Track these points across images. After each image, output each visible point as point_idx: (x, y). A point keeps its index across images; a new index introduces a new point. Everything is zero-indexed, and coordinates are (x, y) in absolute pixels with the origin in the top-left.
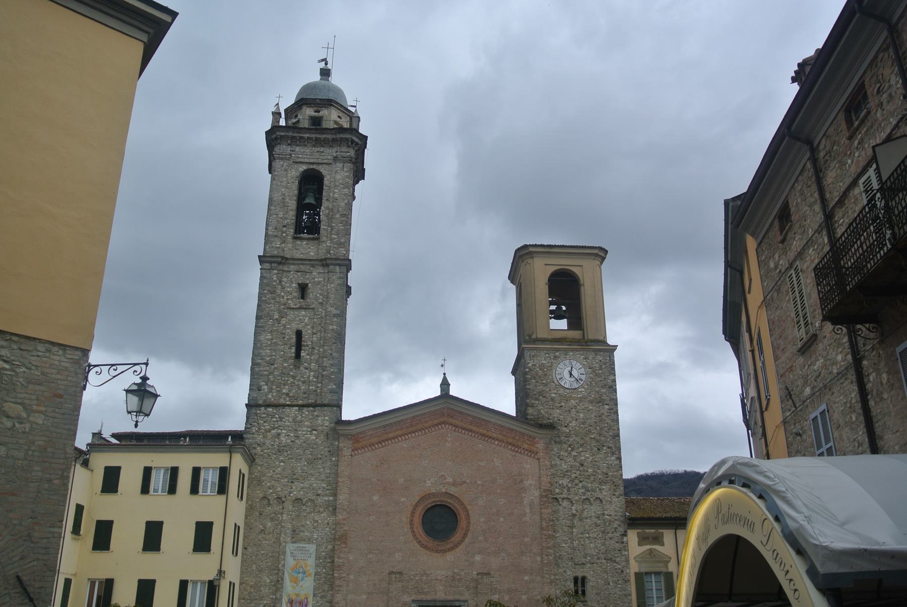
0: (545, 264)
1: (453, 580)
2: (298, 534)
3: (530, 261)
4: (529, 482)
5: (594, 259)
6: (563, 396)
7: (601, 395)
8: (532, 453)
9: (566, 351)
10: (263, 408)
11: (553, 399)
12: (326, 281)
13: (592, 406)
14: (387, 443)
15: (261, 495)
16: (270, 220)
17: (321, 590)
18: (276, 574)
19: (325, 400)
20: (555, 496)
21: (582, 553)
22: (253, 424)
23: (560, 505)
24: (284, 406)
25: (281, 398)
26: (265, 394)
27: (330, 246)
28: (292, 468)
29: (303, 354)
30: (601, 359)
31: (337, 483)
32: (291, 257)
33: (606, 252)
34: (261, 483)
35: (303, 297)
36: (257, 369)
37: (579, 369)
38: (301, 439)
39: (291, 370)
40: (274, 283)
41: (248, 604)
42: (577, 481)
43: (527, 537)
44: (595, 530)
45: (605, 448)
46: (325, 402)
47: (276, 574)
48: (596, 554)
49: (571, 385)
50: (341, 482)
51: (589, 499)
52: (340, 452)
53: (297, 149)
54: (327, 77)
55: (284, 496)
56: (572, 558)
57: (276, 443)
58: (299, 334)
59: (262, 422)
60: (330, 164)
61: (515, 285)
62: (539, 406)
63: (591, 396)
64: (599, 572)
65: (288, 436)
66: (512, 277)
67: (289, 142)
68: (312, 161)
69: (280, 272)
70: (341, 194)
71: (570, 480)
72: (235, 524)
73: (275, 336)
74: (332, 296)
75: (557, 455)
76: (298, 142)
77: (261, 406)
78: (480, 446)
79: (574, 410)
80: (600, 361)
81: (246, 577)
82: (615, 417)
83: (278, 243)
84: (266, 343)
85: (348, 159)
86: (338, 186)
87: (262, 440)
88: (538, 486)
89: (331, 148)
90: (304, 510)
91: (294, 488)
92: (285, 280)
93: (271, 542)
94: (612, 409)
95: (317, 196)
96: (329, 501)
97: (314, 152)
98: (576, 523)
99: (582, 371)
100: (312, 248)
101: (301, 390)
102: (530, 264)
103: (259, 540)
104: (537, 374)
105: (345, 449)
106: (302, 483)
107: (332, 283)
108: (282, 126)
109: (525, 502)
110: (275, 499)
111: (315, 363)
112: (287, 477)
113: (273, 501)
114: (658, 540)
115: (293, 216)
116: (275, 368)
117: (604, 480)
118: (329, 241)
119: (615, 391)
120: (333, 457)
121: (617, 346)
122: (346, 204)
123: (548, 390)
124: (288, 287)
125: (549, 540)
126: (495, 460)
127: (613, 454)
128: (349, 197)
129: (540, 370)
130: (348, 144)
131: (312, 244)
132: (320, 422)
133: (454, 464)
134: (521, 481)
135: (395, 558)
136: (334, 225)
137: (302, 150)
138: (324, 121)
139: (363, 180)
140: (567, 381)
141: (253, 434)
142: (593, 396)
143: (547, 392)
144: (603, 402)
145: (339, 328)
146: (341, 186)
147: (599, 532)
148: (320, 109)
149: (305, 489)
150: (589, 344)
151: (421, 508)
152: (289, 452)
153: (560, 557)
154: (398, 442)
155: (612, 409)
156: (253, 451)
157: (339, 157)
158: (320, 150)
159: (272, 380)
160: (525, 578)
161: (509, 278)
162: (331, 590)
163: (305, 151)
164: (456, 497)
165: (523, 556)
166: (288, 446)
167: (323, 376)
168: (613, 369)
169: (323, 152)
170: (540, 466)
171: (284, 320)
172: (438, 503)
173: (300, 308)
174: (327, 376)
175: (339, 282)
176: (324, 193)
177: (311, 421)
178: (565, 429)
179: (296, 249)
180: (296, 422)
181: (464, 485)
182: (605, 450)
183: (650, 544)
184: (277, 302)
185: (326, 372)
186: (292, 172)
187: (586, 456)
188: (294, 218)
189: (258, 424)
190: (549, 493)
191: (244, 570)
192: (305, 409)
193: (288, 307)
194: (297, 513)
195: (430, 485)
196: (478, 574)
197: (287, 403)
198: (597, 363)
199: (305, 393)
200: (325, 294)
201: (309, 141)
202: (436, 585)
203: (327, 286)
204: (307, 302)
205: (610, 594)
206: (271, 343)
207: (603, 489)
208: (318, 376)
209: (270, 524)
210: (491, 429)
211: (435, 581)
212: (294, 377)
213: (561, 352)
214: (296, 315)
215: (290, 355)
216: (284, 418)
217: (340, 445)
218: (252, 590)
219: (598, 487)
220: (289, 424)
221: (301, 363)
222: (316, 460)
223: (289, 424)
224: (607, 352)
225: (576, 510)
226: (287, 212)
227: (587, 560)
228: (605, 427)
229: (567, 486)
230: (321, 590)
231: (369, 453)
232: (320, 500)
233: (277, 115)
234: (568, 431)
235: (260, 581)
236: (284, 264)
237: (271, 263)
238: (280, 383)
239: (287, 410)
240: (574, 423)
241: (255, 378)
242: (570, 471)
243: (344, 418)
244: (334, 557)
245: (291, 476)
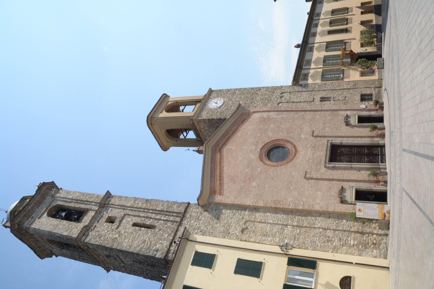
2: (267, 232)
58: (135, 225)
91: (233, 232)
109: (276, 117)
132: (194, 214)
152: (207, 234)
164: (265, 145)
169: (45, 202)
194: (252, 232)
195: (254, 156)
212: (160, 230)
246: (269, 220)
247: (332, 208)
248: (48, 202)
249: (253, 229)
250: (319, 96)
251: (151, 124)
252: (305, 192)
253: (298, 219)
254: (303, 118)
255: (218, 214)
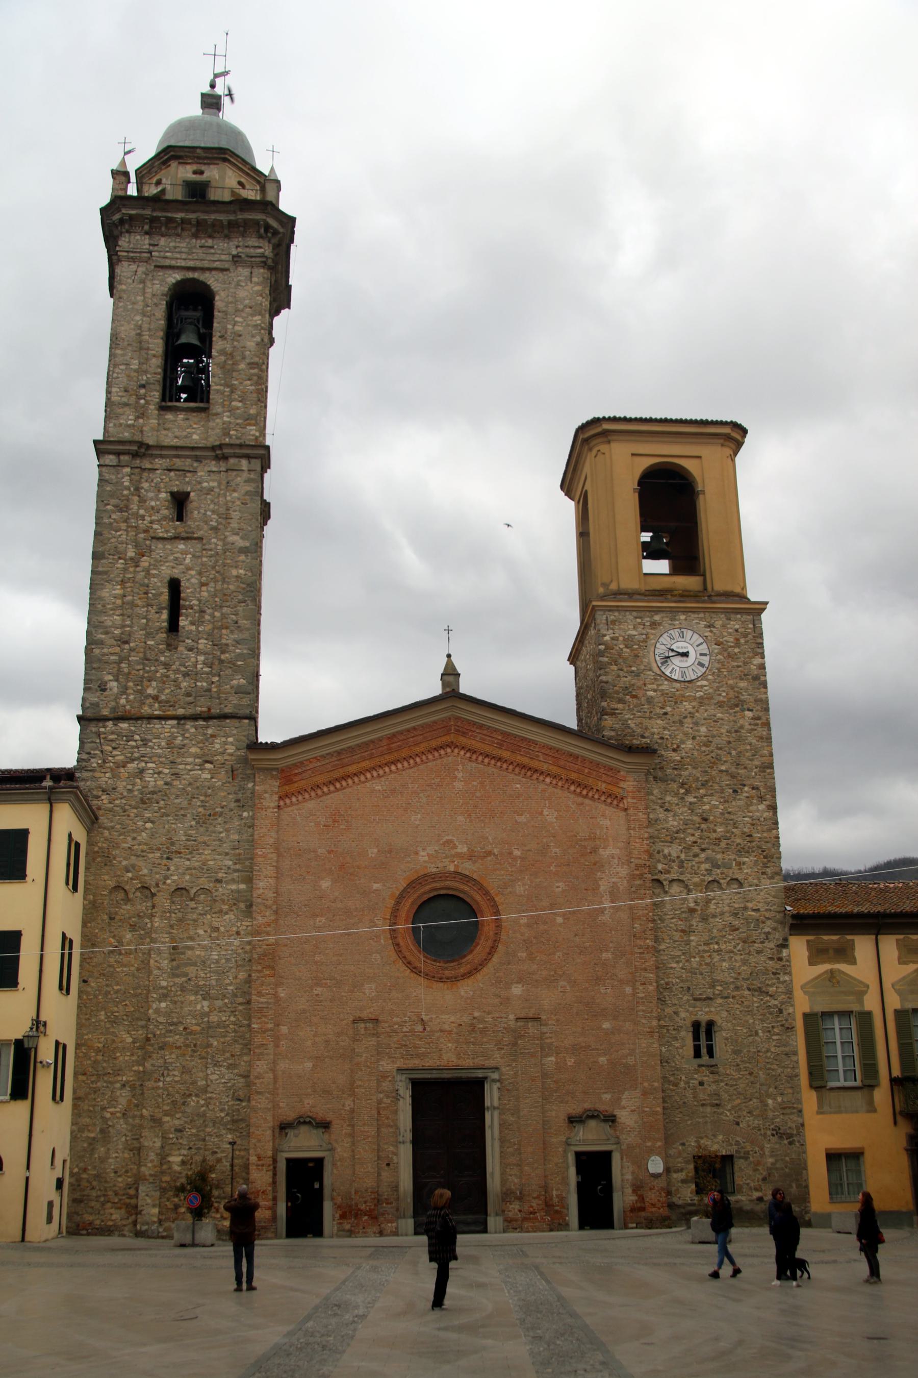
0: (633, 455)
1: (473, 1030)
2: (183, 953)
3: (603, 448)
4: (609, 851)
5: (722, 445)
6: (670, 695)
7: (738, 692)
8: (614, 798)
9: (674, 612)
10: (111, 722)
11: (650, 700)
12: (223, 487)
13: (722, 713)
14: (344, 783)
15: (112, 884)
16: (115, 375)
17: (228, 1055)
18: (142, 1027)
19: (226, 706)
20: (656, 877)
21: (708, 979)
22: (92, 752)
23: (666, 892)
24: (150, 718)
25: (144, 704)
26: (113, 697)
27: (230, 423)
28: (169, 832)
29: (183, 622)
30: (737, 627)
31: (252, 859)
32: (155, 444)
33: (744, 431)
34: (110, 861)
35: (180, 518)
36: (97, 651)
37: (697, 646)
38: (184, 779)
39: (162, 652)
40: (125, 492)
41: (92, 1082)
42: (696, 849)
43: (607, 951)
44: (731, 937)
45: (746, 789)
46: (228, 710)
47: (142, 1027)
48: (732, 980)
49: (683, 674)
50: (261, 856)
51: (718, 882)
52: (257, 801)
53: (163, 241)
54: (215, 111)
55: (154, 883)
56: (689, 988)
57: (136, 788)
58: (174, 586)
59: (110, 748)
60: (227, 270)
61: (573, 500)
62: (625, 712)
63: (720, 695)
64: (738, 1013)
65: (159, 773)
66: (568, 486)
67: (147, 227)
68: (191, 264)
69: (137, 470)
70: (248, 325)
71: (684, 848)
72: (64, 934)
73: (129, 590)
74: (235, 515)
75: (659, 801)
76: (163, 229)
77: (106, 719)
78: (518, 786)
79: (689, 720)
80: (737, 631)
81: (87, 1035)
82: (764, 733)
83: (130, 417)
84: (114, 603)
85: (258, 259)
86: (242, 311)
87: (109, 781)
88: (626, 858)
89: (226, 241)
90: (192, 909)
91: (172, 868)
92: (145, 485)
93: (133, 969)
94: (759, 718)
95: (202, 331)
96: (238, 891)
97: (195, 247)
98: (695, 924)
99: (704, 648)
100: (195, 426)
101: (181, 688)
102: (604, 454)
103: (110, 966)
104: (620, 655)
105: (266, 795)
106: (188, 860)
107: (234, 491)
108: (131, 197)
109: (602, 888)
110: (137, 889)
111: (206, 639)
112: (159, 849)
113: (134, 893)
114: (845, 953)
115: (158, 367)
116: (132, 650)
117: (746, 847)
118: (228, 414)
119: (764, 685)
120: (244, 811)
121: (767, 603)
122: (257, 344)
123: (640, 683)
124: (152, 499)
125: (647, 956)
126: (546, 812)
127: (761, 799)
128: (263, 331)
129: (627, 647)
130: (258, 231)
131: (196, 420)
132: (217, 746)
133: (471, 821)
134: (594, 850)
135: (364, 993)
136: (235, 382)
137: (172, 244)
138: (213, 190)
139: (287, 310)
140: (676, 668)
141: (93, 771)
142: (724, 694)
143: (639, 688)
144: (742, 706)
145: (250, 574)
146: (248, 310)
147: (738, 941)
148: (203, 168)
149: (194, 871)
150: (714, 598)
151: (408, 904)
152: (162, 802)
153: (668, 987)
154: (364, 782)
155: (759, 718)
156: (95, 803)
157: (243, 256)
158: (207, 244)
159: (126, 670)
160: (604, 1026)
161: (562, 487)
162: (246, 1054)
163: (178, 245)
165: (599, 985)
166: (160, 791)
167: (221, 662)
168: (762, 645)
169: (212, 247)
170: (629, 821)
171: (145, 561)
172: (442, 892)
173: (176, 538)
174: (229, 662)
175: (248, 488)
176: (215, 325)
177: (201, 745)
178: (673, 754)
179: (165, 429)
180: (173, 748)
181: (489, 858)
182: (746, 792)
183: (829, 962)
184: (132, 527)
185: (227, 655)
186: (154, 284)
187: (713, 804)
188: (159, 370)
189: (102, 752)
190: (646, 871)
191: (84, 1021)
192: (189, 725)
193: (153, 535)
194: (180, 915)
196: (518, 1019)
197: (156, 713)
198: (730, 634)
199: (188, 695)
200: (222, 510)
201: (185, 226)
202: (442, 1040)
203: (225, 496)
204: (189, 526)
205: (759, 1051)
206: (123, 603)
207: (744, 864)
208: (212, 664)
209: (129, 936)
210: (538, 756)
211: (439, 1034)
212: (167, 666)
213: (664, 615)
214: (169, 552)
215: (158, 624)
216: (151, 741)
217: (257, 788)
218: (100, 1058)
219: (735, 860)
220: (160, 751)
221: (181, 639)
222: (212, 818)
223: (160, 751)
224: (748, 614)
225: (695, 902)
226: (147, 359)
227: (717, 992)
228: (747, 751)
229: (678, 857)
230: (228, 1055)
231: (313, 802)
232: (222, 890)
233: (120, 175)
234: (678, 758)
235: (114, 1041)
236: (144, 456)
237: (118, 454)
238: (143, 677)
239: (157, 725)
240: (689, 744)
241: (94, 668)
242: (684, 831)
243: (263, 738)
244: (250, 994)
245: (167, 848)
246: (219, 950)
247: (260, 1103)
248: (216, 257)
249: (190, 916)
250: (724, 1014)
251: (586, 441)
252: (309, 1029)
253: (227, 1023)
254: (597, 978)
255: (226, 810)
